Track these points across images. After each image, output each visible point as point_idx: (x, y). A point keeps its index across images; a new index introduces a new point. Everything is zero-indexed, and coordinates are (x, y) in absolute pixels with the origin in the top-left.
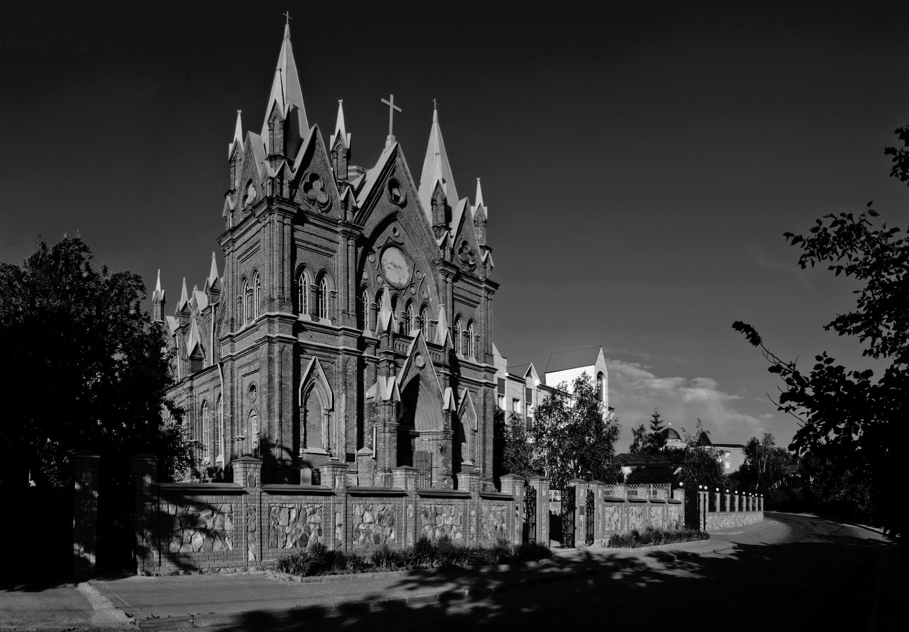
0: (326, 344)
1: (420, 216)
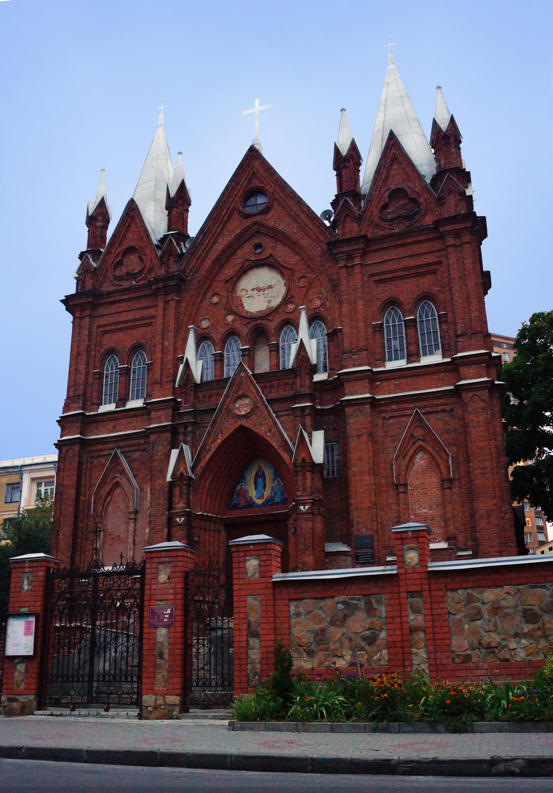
0: (135, 429)
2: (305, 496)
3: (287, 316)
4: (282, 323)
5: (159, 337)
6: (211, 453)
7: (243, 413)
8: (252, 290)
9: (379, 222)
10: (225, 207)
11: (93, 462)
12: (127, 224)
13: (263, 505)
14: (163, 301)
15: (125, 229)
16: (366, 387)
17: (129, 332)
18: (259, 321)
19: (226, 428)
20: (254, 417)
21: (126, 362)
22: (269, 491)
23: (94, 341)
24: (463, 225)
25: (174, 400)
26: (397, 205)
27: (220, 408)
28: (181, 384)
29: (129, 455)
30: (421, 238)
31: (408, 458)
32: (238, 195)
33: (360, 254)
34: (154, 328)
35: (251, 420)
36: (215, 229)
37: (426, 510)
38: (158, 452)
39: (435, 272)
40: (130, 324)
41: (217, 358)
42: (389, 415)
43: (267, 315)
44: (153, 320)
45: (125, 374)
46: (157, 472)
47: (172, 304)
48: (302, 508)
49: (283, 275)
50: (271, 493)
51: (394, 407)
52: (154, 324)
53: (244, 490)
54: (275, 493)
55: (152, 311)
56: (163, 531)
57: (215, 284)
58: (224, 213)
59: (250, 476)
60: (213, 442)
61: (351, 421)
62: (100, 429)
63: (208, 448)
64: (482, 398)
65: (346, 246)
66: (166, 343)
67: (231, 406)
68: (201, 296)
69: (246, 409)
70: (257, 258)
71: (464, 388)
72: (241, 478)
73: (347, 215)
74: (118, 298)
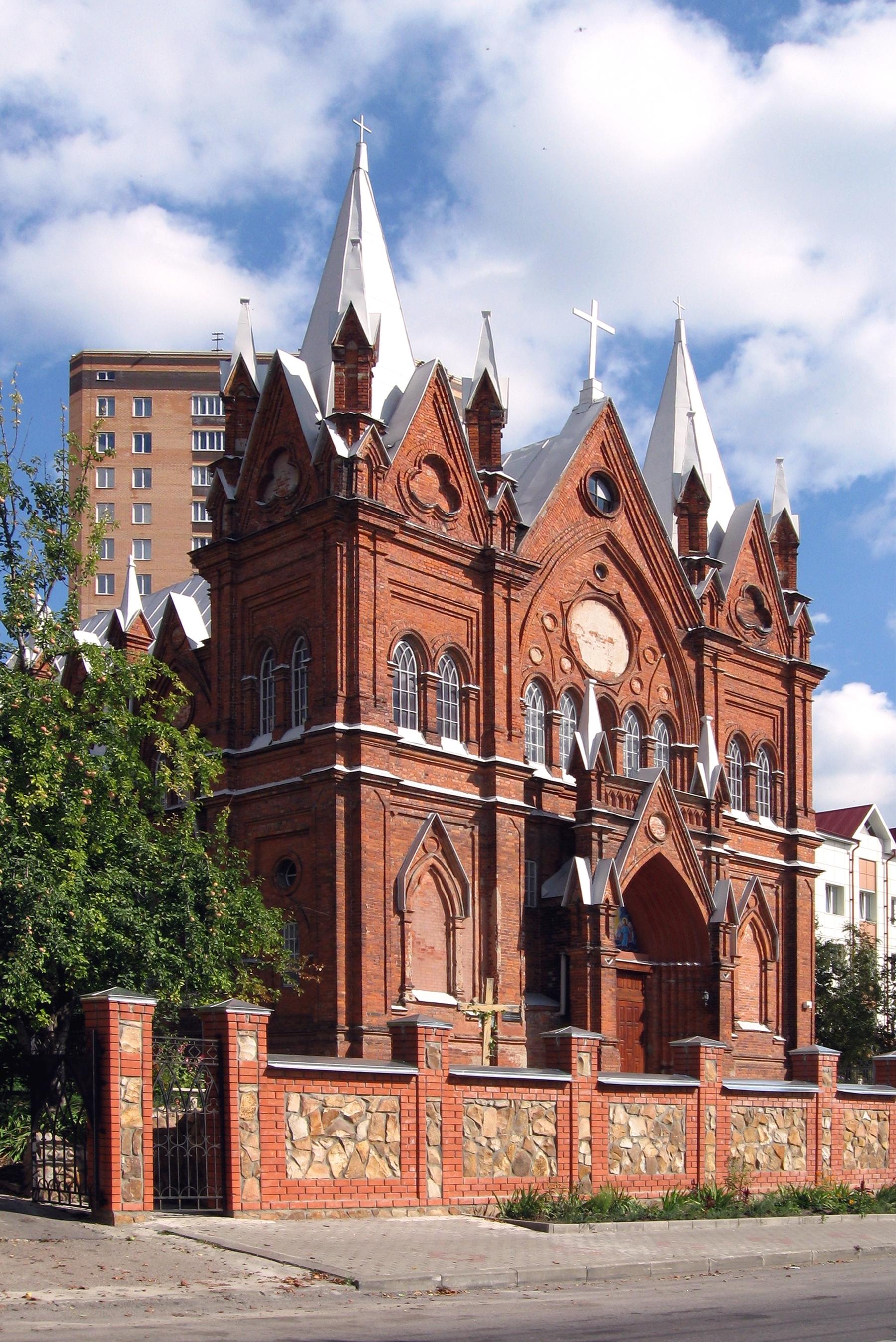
0: (458, 789)
38: (506, 840)
40: (439, 603)
74: (426, 547)
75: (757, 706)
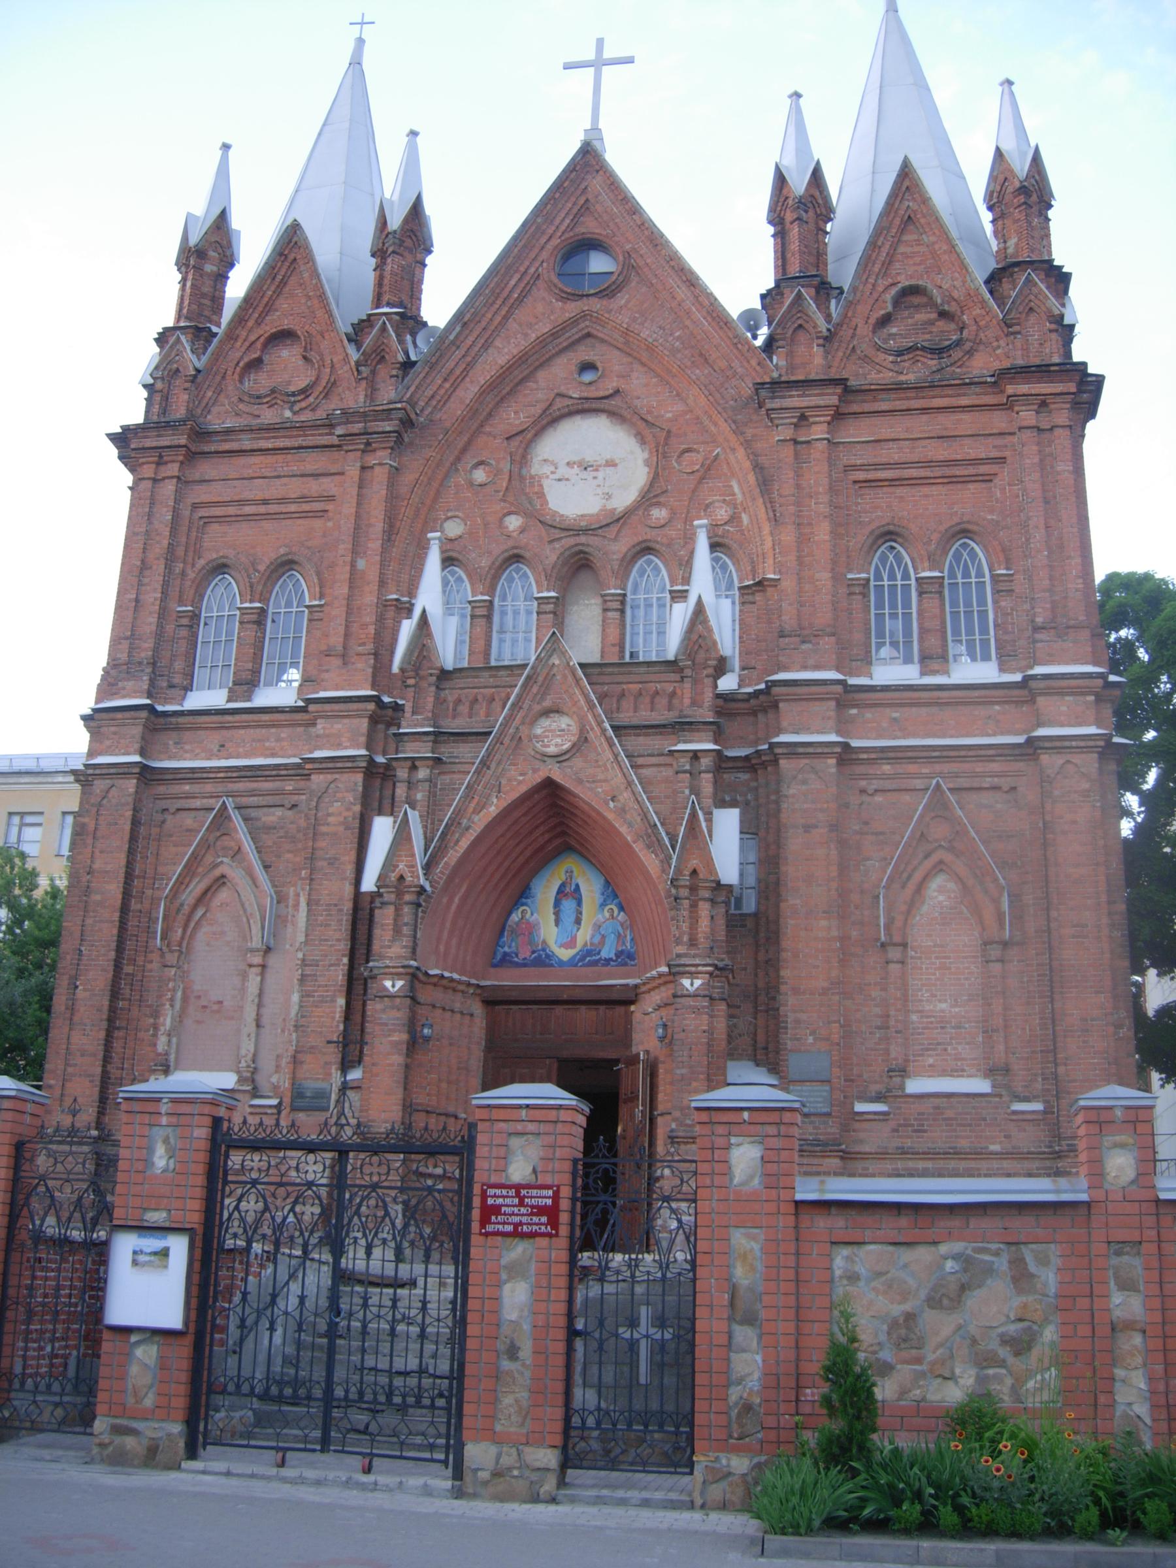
0: (273, 755)
1: (682, 293)
2: (694, 956)
3: (650, 534)
4: (638, 548)
5: (344, 547)
6: (472, 835)
7: (552, 750)
8: (568, 464)
9: (871, 352)
10: (516, 272)
11: (163, 822)
12: (279, 277)
13: (572, 963)
14: (359, 464)
15: (273, 288)
16: (829, 718)
17: (266, 525)
18: (583, 539)
19: (510, 780)
20: (578, 762)
21: (257, 596)
22: (590, 932)
23: (184, 539)
24: (1059, 388)
25: (377, 700)
26: (910, 321)
27: (501, 732)
28: (405, 666)
29: (253, 813)
30: (964, 401)
31: (912, 885)
32: (549, 246)
33: (829, 418)
34: (330, 524)
35: (571, 767)
36: (489, 316)
37: (944, 1006)
38: (329, 815)
39: (988, 479)
40: (273, 508)
41: (479, 612)
42: (875, 784)
43: (601, 528)
44: (330, 507)
45: (254, 622)
46: (325, 864)
47: (380, 476)
48: (686, 982)
49: (642, 440)
50: (593, 936)
51: (887, 768)
52: (330, 514)
53: (528, 923)
54: (603, 937)
55: (328, 485)
56: (333, 1001)
57: (481, 440)
58: (513, 282)
59: (545, 889)
60: (477, 811)
61: (791, 792)
62: (187, 747)
63: (465, 822)
64: (1083, 770)
65: (799, 396)
66: (361, 564)
67: (524, 731)
68: (448, 464)
69: (559, 740)
70: (585, 395)
71: (1047, 745)
72: (522, 894)
73: (800, 326)
74: (247, 445)
75: (938, 472)
